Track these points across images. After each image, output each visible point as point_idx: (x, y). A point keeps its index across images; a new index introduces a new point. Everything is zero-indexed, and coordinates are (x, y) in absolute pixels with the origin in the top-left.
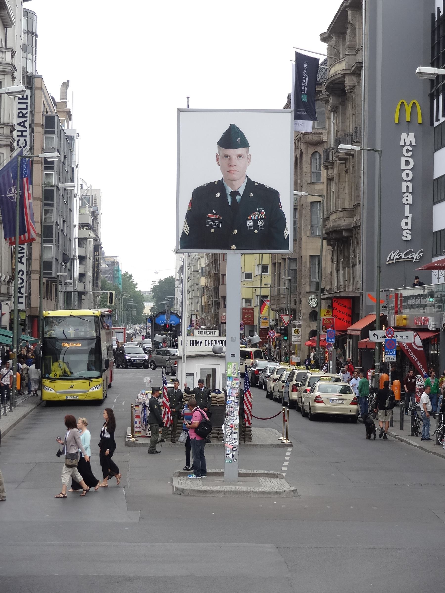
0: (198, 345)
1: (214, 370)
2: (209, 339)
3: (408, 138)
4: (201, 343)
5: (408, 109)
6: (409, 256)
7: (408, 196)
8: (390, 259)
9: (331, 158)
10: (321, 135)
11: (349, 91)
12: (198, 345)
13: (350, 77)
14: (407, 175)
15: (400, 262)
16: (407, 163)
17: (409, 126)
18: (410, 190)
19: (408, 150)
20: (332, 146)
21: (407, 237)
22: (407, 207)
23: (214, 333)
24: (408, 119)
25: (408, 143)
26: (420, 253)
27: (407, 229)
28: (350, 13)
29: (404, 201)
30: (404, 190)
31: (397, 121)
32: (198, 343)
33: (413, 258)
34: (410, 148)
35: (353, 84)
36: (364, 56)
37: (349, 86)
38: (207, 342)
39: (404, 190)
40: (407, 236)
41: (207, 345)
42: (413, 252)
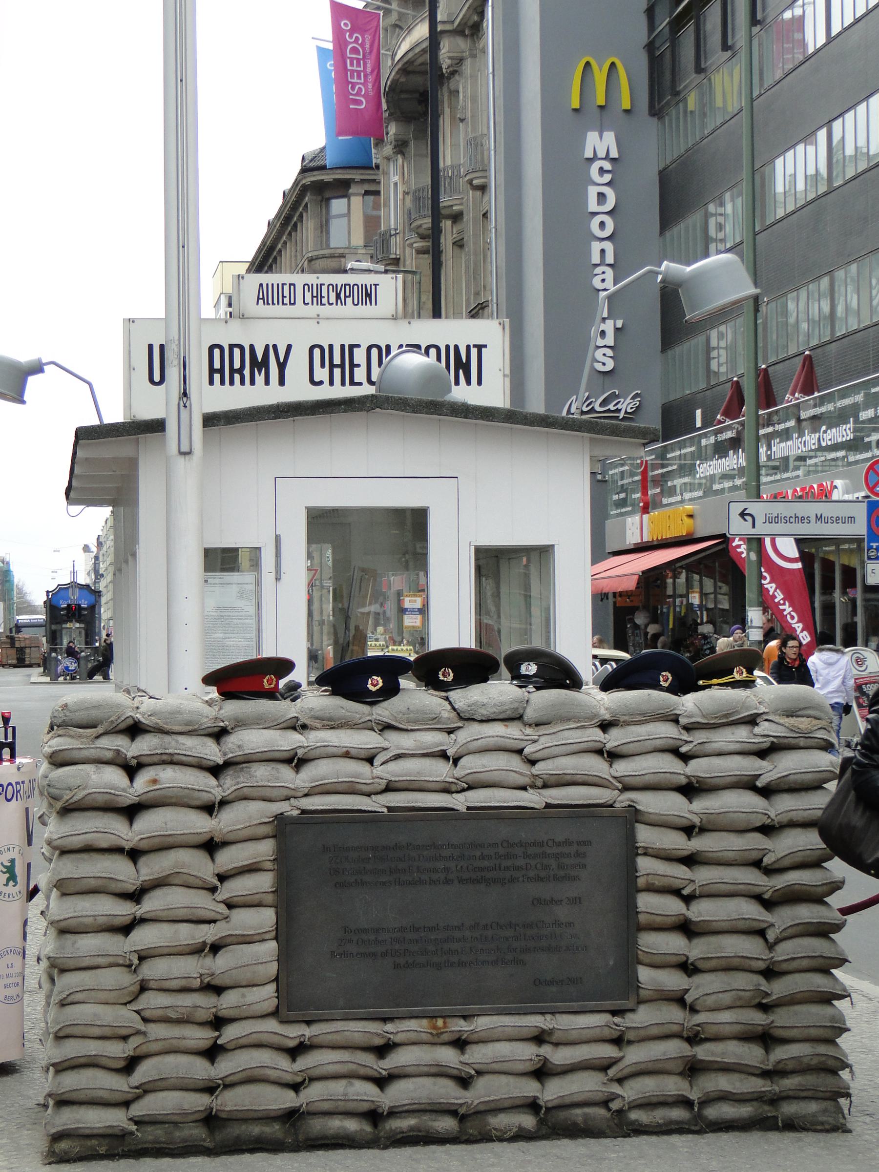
0: (260, 379)
1: (413, 524)
2: (336, 335)
4: (282, 367)
5: (600, 77)
7: (603, 273)
9: (393, 250)
10: (343, 260)
11: (451, 69)
12: (260, 379)
13: (452, 39)
18: (610, 259)
19: (601, 169)
20: (392, 227)
21: (604, 364)
23: (368, 295)
24: (601, 101)
25: (602, 154)
26: (633, 398)
27: (605, 346)
29: (597, 283)
30: (596, 258)
31: (576, 104)
32: (260, 364)
34: (607, 166)
35: (459, 55)
37: (450, 58)
38: (319, 353)
39: (596, 258)
41: (321, 374)
42: (618, 397)
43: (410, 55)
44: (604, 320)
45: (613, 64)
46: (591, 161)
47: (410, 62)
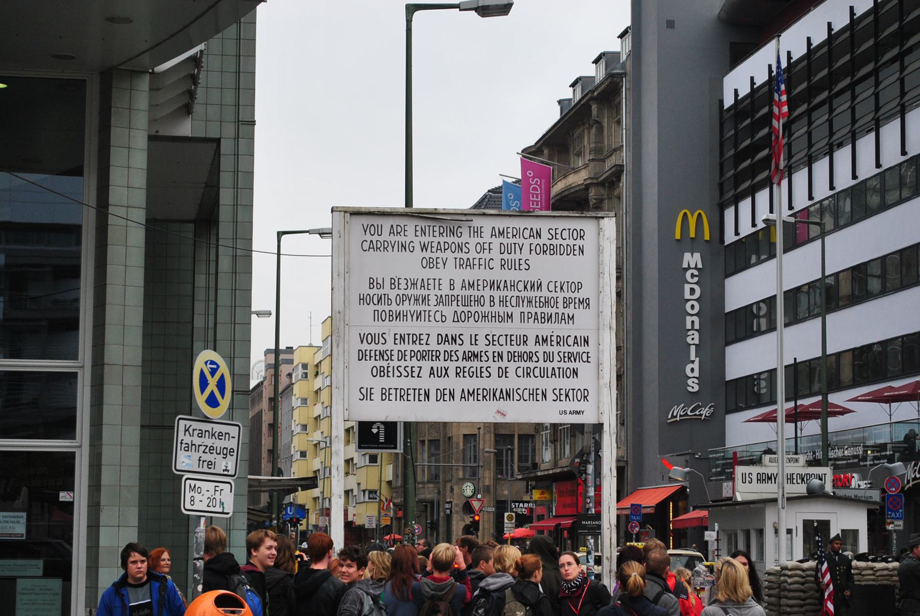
3: (693, 260)
5: (692, 221)
6: (697, 413)
8: (673, 417)
14: (693, 307)
15: (685, 421)
16: (692, 291)
17: (693, 245)
18: (697, 326)
22: (693, 348)
23: (797, 461)
25: (692, 266)
28: (594, 108)
29: (689, 340)
30: (689, 326)
31: (678, 236)
33: (701, 415)
34: (696, 273)
36: (625, 157)
39: (689, 326)
40: (693, 386)
43: (567, 193)
44: (693, 362)
45: (700, 214)
46: (686, 269)
47: (566, 196)
